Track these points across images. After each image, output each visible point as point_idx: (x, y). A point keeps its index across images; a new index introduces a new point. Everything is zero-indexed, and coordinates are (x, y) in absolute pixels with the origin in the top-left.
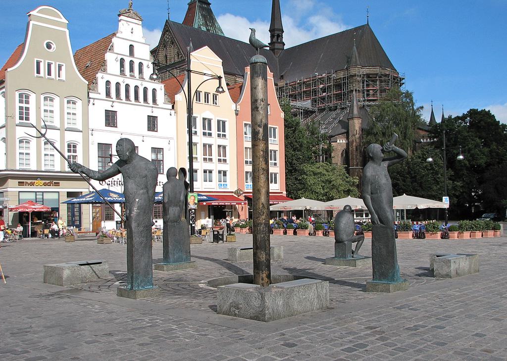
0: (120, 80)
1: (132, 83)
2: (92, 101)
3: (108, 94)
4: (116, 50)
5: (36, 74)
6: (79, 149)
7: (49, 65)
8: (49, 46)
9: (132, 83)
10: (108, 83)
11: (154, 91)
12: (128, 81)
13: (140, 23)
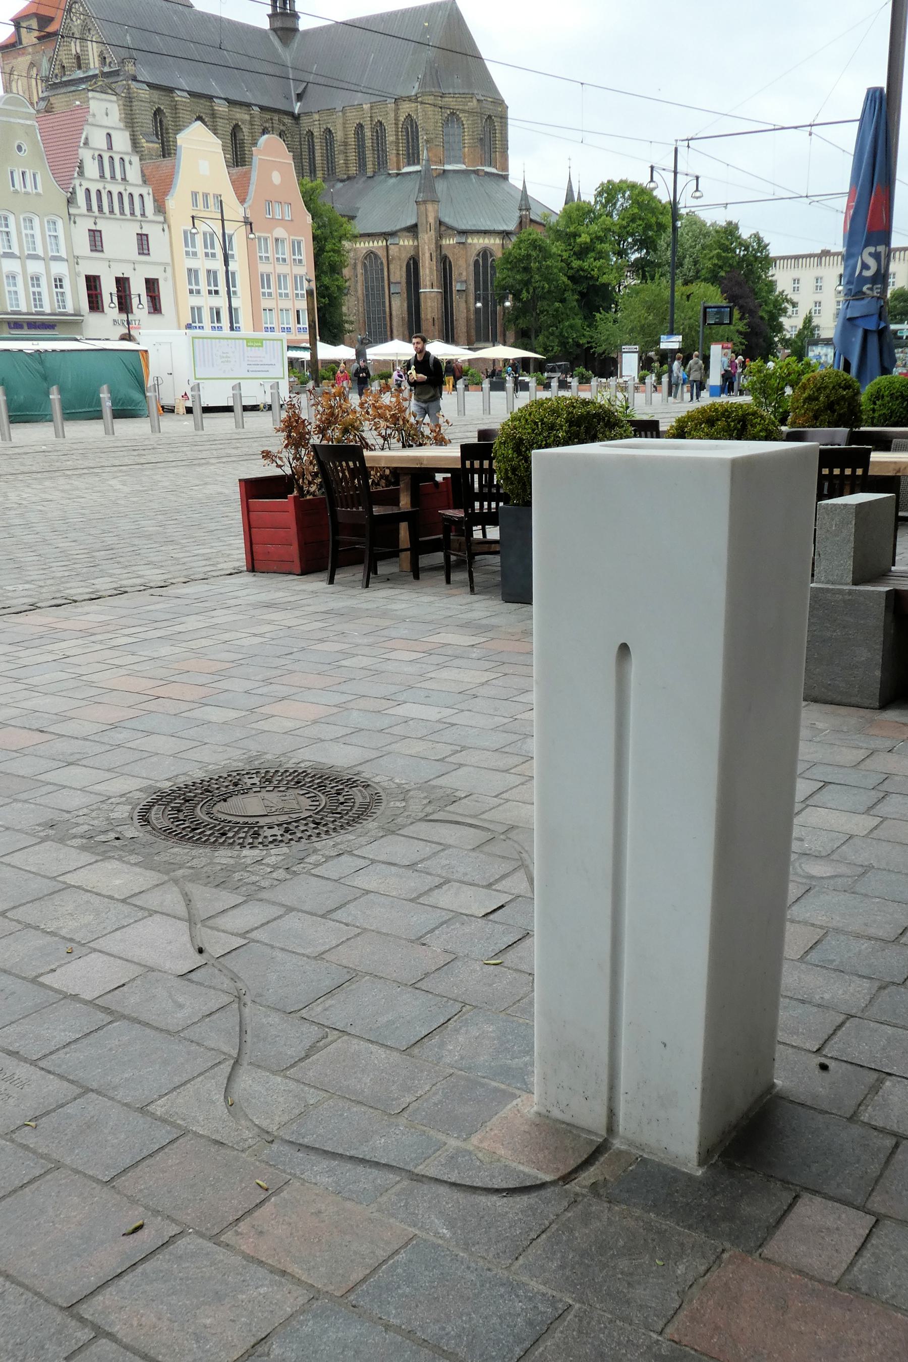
0: (100, 186)
1: (115, 189)
2: (72, 218)
3: (89, 209)
4: (92, 143)
5: (12, 188)
6: (66, 283)
7: (23, 173)
8: (19, 148)
9: (115, 189)
10: (88, 191)
11: (141, 195)
12: (109, 187)
13: (114, 98)
